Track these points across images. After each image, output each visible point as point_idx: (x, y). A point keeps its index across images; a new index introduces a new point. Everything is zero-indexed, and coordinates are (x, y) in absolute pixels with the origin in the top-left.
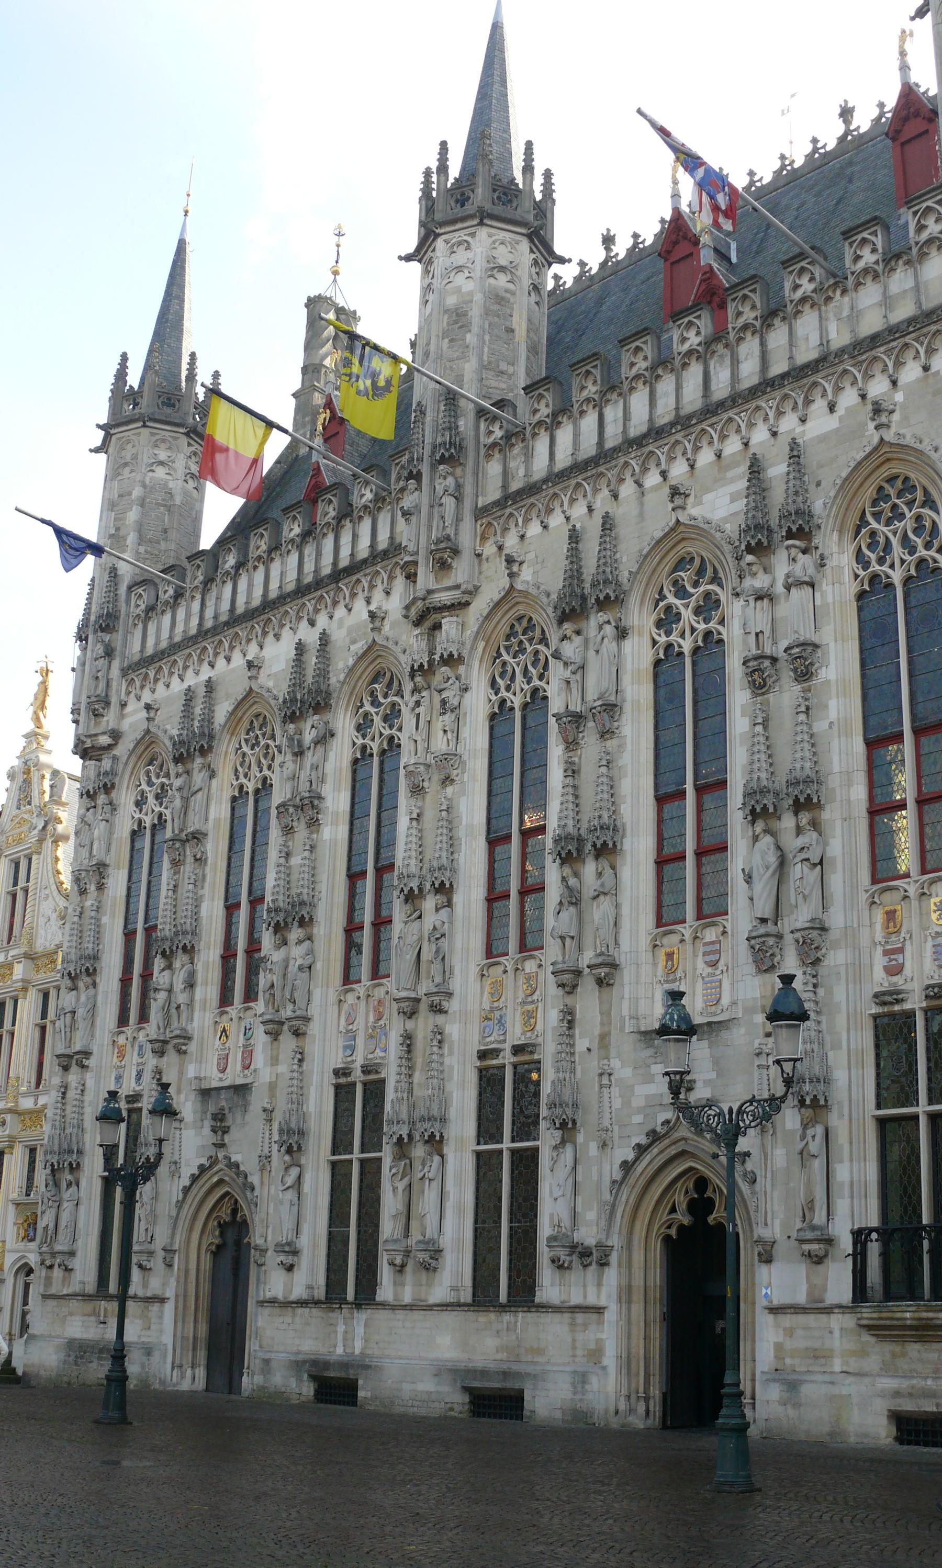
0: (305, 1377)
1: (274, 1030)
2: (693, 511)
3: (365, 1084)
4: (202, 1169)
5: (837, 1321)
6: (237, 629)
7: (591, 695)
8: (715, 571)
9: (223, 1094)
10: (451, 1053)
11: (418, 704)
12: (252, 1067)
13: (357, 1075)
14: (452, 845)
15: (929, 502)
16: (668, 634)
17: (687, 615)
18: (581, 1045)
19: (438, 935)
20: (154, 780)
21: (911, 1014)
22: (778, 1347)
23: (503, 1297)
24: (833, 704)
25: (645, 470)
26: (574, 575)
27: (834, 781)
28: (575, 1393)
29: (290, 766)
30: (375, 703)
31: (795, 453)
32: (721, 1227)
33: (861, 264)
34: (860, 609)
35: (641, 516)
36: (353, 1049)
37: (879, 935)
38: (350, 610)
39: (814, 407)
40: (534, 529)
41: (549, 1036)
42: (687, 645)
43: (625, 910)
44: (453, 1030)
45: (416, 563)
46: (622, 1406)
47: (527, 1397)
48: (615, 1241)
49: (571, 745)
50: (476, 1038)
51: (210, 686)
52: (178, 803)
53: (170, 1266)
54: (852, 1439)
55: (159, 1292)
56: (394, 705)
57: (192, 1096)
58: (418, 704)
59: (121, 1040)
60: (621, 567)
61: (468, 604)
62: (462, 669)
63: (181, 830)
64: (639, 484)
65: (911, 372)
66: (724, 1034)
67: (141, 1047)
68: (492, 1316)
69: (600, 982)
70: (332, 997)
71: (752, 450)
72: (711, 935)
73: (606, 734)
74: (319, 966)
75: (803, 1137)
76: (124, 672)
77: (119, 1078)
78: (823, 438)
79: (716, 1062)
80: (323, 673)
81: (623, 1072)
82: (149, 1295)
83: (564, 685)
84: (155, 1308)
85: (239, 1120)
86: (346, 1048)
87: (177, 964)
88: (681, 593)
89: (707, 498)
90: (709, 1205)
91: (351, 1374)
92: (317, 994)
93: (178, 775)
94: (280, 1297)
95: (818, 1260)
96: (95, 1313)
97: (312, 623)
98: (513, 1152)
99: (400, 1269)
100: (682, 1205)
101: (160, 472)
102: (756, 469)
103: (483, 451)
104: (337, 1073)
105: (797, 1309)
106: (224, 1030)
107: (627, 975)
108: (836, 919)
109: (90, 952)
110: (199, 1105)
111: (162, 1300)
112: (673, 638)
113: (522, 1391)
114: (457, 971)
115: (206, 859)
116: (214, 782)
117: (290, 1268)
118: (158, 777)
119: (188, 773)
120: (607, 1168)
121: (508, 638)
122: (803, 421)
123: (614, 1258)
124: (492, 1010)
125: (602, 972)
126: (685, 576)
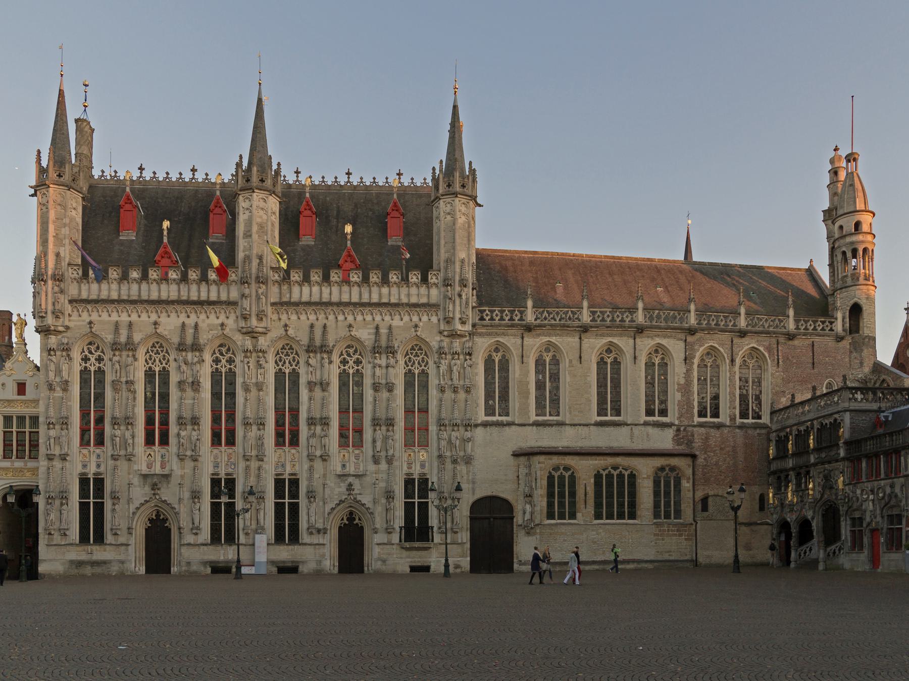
0: (208, 566)
1: (181, 458)
2: (356, 333)
3: (225, 479)
4: (146, 502)
5: (394, 547)
7: (318, 377)
8: (360, 353)
9: (155, 477)
10: (266, 472)
11: (248, 362)
12: (167, 468)
13: (223, 476)
14: (265, 411)
15: (426, 354)
16: (344, 366)
17: (351, 363)
18: (316, 476)
19: (260, 438)
20: (94, 352)
21: (415, 479)
22: (379, 552)
23: (287, 542)
24: (398, 400)
25: (339, 314)
26: (312, 339)
27: (397, 420)
28: (317, 565)
29: (184, 367)
30: (222, 354)
31: (390, 328)
32: (357, 524)
33: (413, 280)
34: (405, 377)
35: (337, 327)
36: (218, 467)
37: (406, 459)
38: (208, 317)
39: (396, 317)
40: (294, 317)
41: (304, 472)
42: (351, 371)
43: (331, 442)
44: (265, 466)
45: (250, 315)
46: (332, 568)
47: (301, 568)
48: (329, 528)
49: (311, 390)
50: (273, 469)
51: (130, 325)
52: (117, 366)
53: (131, 534)
54: (400, 572)
55: (126, 543)
56: (230, 357)
57: (138, 476)
58: (248, 362)
59: (85, 451)
60: (329, 342)
61: (265, 334)
62: (265, 355)
63: (120, 377)
64: (336, 318)
65: (425, 318)
66: (364, 478)
67: (98, 456)
68: (286, 547)
69: (324, 460)
70: (210, 450)
71: (376, 323)
72: (357, 452)
74: (203, 439)
75: (389, 505)
76: (71, 302)
77: (85, 466)
78: (398, 327)
79: (361, 484)
80: (196, 337)
81: (332, 485)
82: (119, 543)
84: (123, 548)
85: (165, 485)
86: (214, 467)
87: (123, 428)
88: (349, 355)
89: (359, 330)
90: (354, 519)
91: (230, 565)
92: (202, 448)
93: (114, 355)
94: (192, 543)
95: (390, 533)
96: (84, 551)
97: (188, 317)
98: (289, 503)
99: (247, 534)
100: (345, 518)
101: (74, 213)
102: (377, 328)
103: (272, 283)
104: (213, 474)
105: (384, 544)
106: (150, 454)
107: (332, 458)
108: (397, 454)
109: (65, 416)
110: (142, 480)
111: (127, 545)
112: (346, 367)
113: (298, 566)
114: (267, 449)
115: (135, 392)
116: (136, 363)
117: (196, 534)
118: (96, 351)
119: (120, 356)
120: (326, 509)
121: (282, 349)
122: (392, 320)
123: (328, 532)
124: (278, 462)
125: (327, 458)
126: (351, 351)
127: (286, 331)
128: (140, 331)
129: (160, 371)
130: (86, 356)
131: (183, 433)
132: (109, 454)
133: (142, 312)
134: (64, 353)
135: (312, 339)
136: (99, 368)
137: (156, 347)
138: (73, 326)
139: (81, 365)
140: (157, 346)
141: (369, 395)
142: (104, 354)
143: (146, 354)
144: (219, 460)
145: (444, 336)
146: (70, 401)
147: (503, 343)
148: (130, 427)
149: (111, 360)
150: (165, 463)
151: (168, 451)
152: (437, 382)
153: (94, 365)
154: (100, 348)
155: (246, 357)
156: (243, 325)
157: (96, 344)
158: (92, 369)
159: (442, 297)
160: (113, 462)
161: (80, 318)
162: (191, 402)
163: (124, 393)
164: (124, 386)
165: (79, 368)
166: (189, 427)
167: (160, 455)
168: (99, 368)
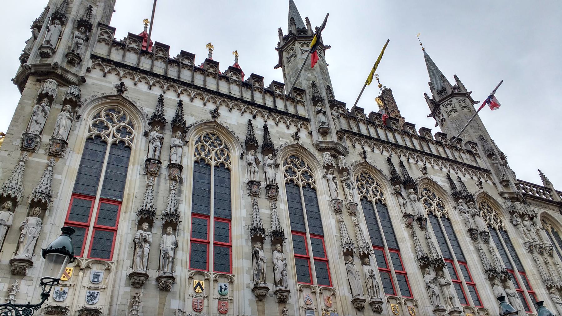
6: (201, 92)
26: (393, 172)
38: (277, 125)
49: (410, 226)
51: (180, 104)
52: (158, 143)
56: (306, 172)
58: (334, 178)
67: (97, 276)
73: (423, 228)
76: (94, 57)
83: (402, 204)
93: (151, 130)
106: (199, 283)
115: (181, 182)
116: (185, 149)
118: (119, 121)
127: (365, 158)
128: (192, 115)
129: (216, 166)
130: (102, 122)
131: (261, 254)
132: (125, 272)
133: (195, 97)
134: (68, 107)
135: (393, 172)
136: (122, 142)
137: (210, 138)
138: (90, 83)
139: (90, 131)
140: (213, 138)
141: (469, 243)
142: (132, 126)
143: (197, 142)
144: (313, 306)
145: (505, 198)
146: (61, 174)
147: (550, 215)
148: (170, 229)
149: (146, 134)
150: (227, 305)
151: (231, 282)
152: (521, 241)
153: (114, 136)
154: (128, 120)
155: (327, 173)
156: (320, 140)
157: (122, 113)
158: (110, 140)
159: (488, 164)
160: (128, 289)
161: (103, 78)
162: (268, 212)
163: (162, 181)
164: (164, 171)
165: (87, 135)
166: (267, 245)
167: (217, 289)
168: (122, 142)
